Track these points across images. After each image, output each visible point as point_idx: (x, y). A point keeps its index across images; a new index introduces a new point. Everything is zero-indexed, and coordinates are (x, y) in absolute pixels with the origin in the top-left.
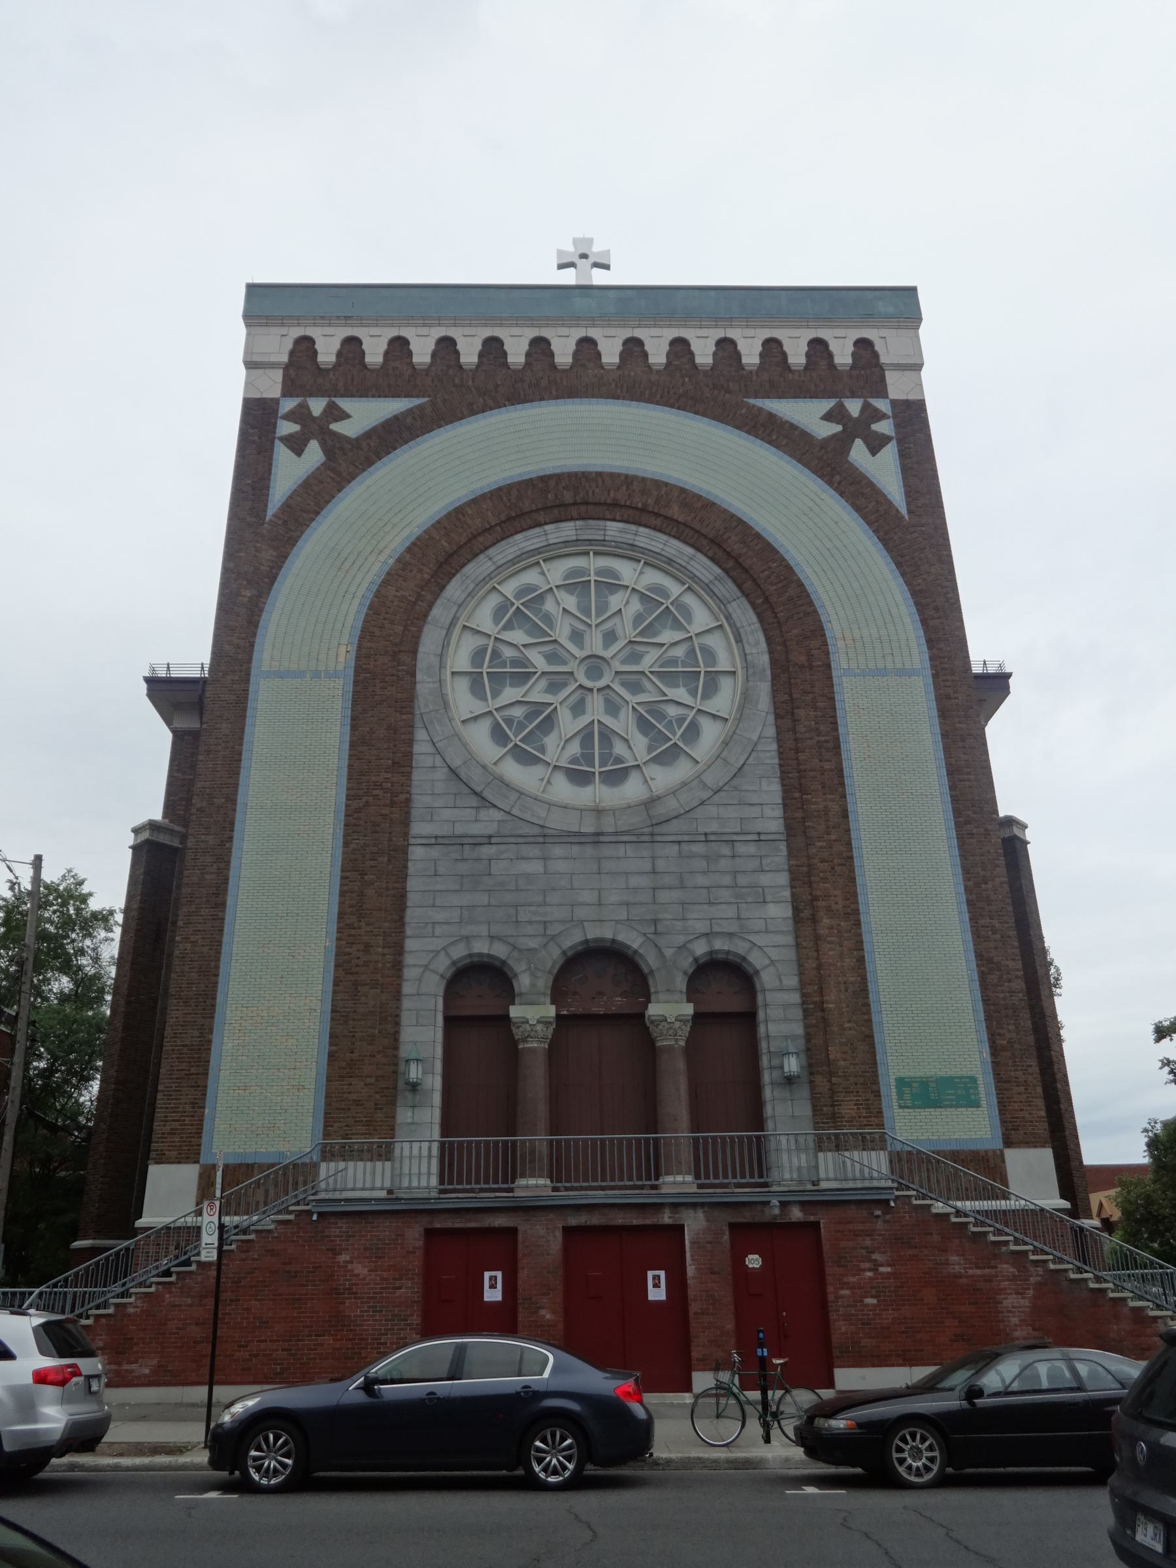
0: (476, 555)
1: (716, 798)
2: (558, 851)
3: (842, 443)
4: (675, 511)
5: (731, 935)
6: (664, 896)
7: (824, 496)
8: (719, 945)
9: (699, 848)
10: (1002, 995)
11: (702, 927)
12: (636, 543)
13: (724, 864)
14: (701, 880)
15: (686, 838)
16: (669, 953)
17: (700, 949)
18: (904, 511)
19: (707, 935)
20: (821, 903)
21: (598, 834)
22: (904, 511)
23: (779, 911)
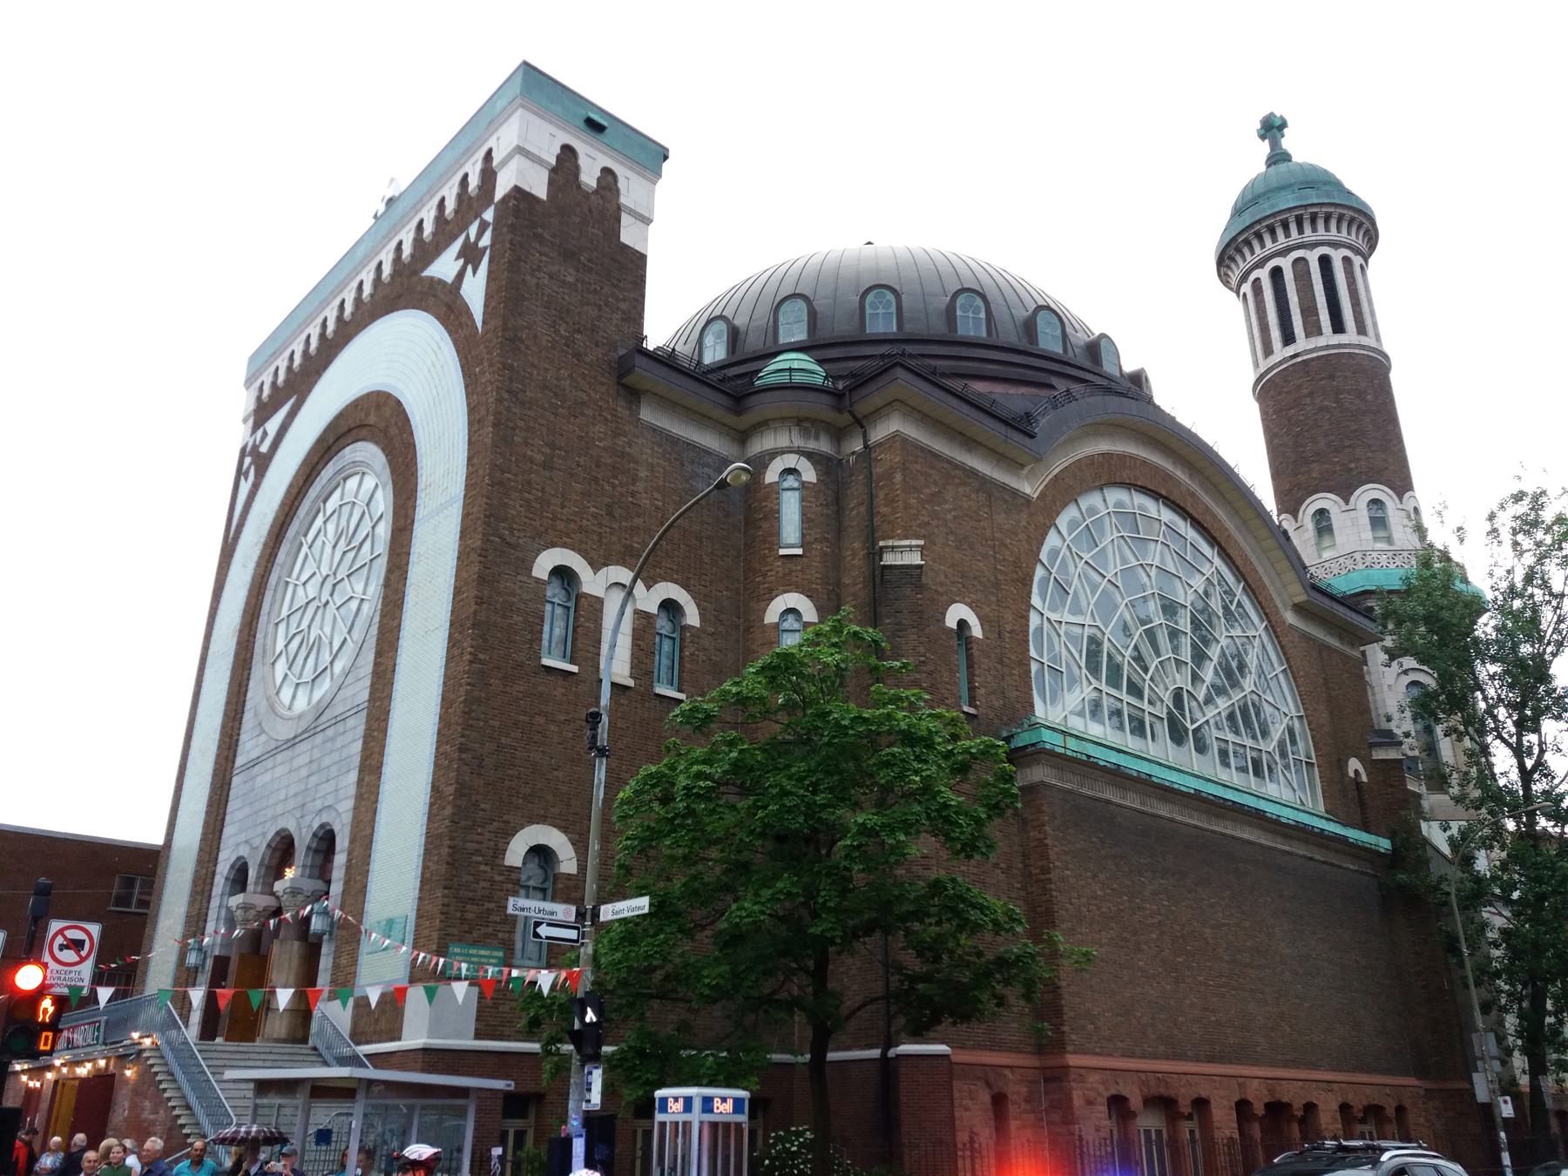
0: (292, 519)
1: (348, 681)
2: (279, 758)
3: (460, 276)
4: (372, 420)
5: (330, 806)
6: (313, 780)
7: (442, 344)
8: (325, 818)
9: (330, 732)
10: (436, 825)
11: (319, 804)
12: (357, 459)
13: (338, 743)
14: (327, 761)
15: (328, 724)
16: (304, 830)
17: (316, 825)
18: (479, 325)
19: (320, 810)
20: (368, 762)
21: (295, 737)
22: (479, 325)
23: (353, 776)
